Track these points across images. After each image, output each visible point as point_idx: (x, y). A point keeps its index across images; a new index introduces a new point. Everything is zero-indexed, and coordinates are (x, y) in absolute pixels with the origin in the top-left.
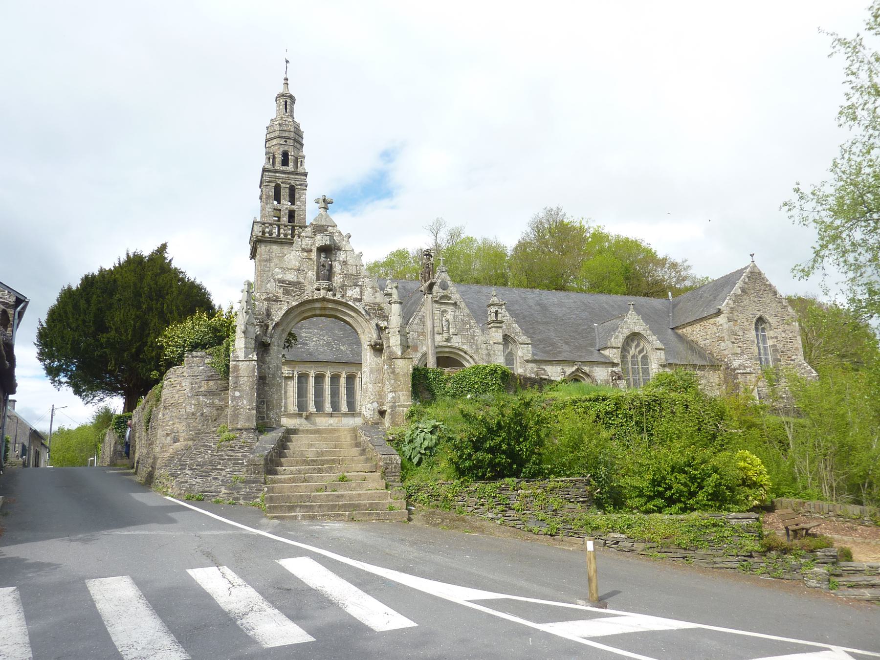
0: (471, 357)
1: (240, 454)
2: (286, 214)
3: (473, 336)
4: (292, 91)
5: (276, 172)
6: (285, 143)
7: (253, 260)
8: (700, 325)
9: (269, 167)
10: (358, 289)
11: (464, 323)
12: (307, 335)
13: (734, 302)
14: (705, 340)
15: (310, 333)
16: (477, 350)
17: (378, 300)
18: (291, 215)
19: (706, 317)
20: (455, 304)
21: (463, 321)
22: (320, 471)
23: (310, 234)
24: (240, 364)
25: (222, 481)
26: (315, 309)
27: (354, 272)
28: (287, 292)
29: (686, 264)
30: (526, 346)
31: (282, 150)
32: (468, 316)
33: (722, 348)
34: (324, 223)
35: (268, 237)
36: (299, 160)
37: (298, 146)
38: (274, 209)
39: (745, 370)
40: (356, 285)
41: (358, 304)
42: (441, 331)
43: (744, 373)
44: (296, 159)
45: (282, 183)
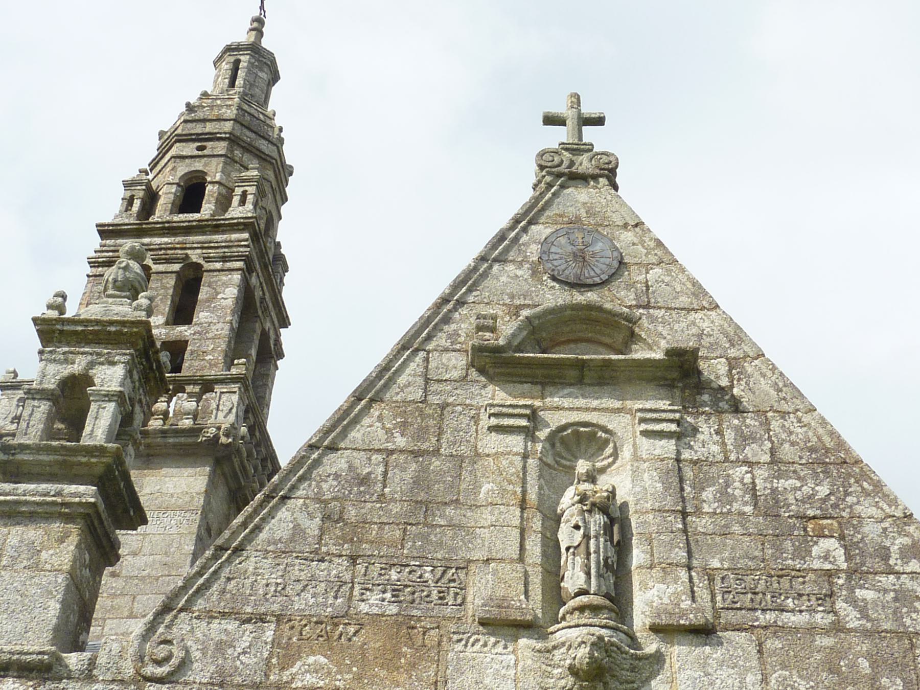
45: (156, 261)
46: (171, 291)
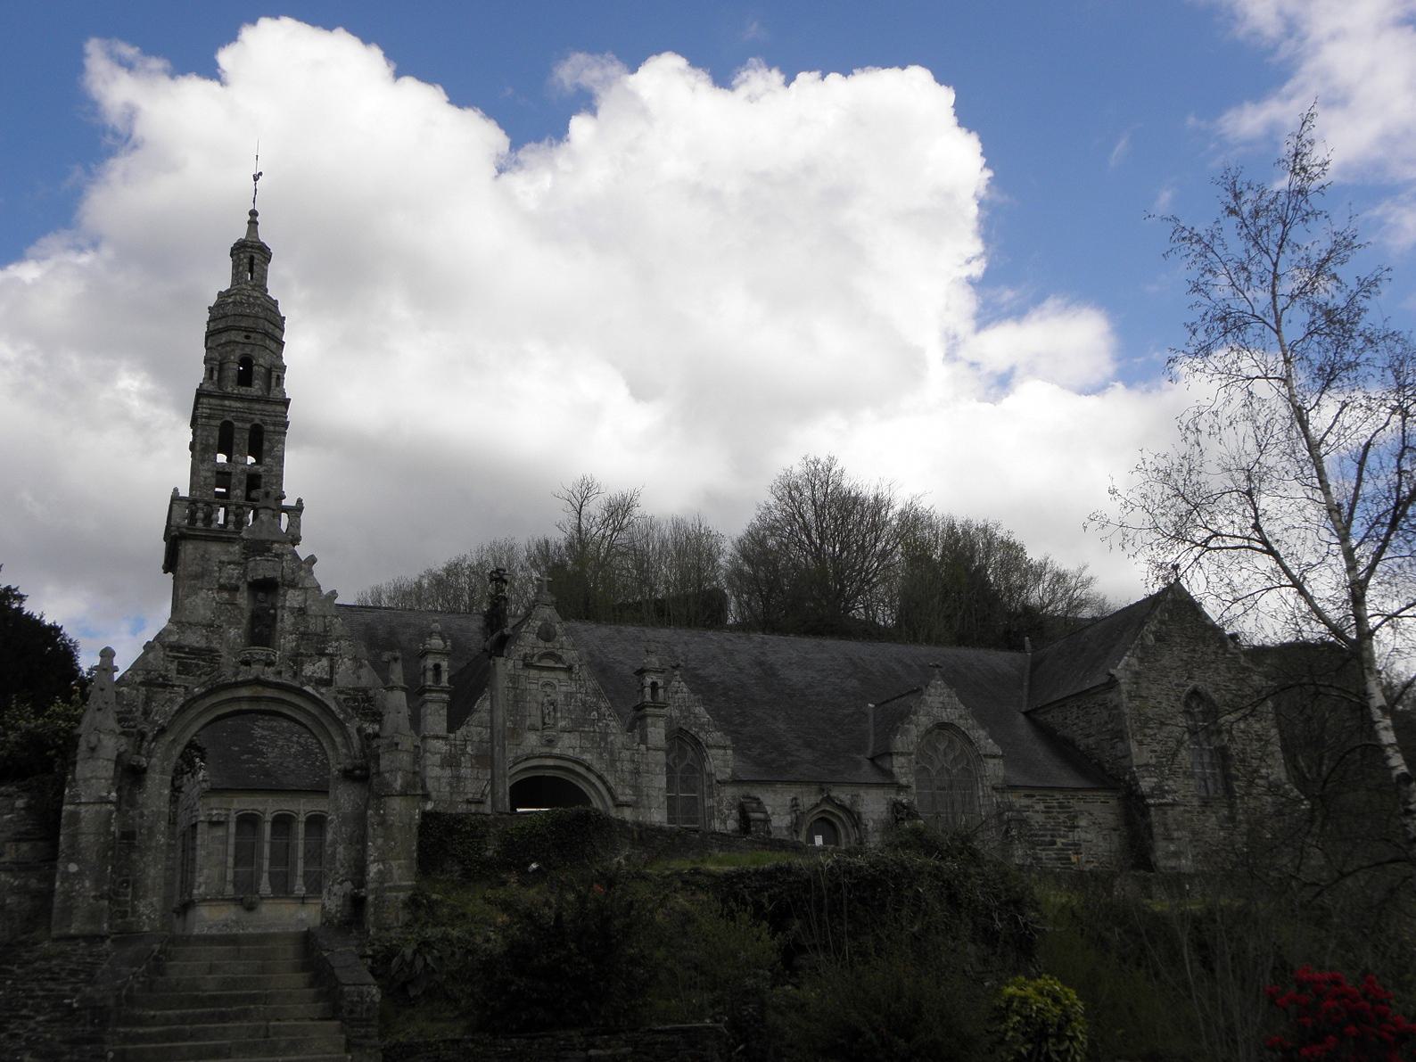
0: (600, 777)
1: (68, 987)
2: (240, 483)
3: (604, 736)
4: (264, 236)
5: (225, 397)
6: (246, 341)
7: (170, 575)
8: (1078, 707)
9: (209, 387)
10: (325, 662)
11: (586, 707)
12: (265, 733)
13: (1141, 660)
14: (1088, 736)
15: (272, 729)
16: (613, 762)
17: (364, 683)
18: (253, 481)
19: (1088, 690)
20: (569, 669)
21: (584, 704)
22: (223, 1017)
23: (236, 558)
24: (83, 809)
25: (28, 1039)
26: (239, 699)
27: (320, 629)
28: (184, 669)
29: (1086, 575)
30: (721, 752)
31: (238, 353)
32: (596, 693)
33: (1119, 754)
34: (264, 536)
35: (201, 530)
36: (274, 375)
37: (273, 346)
38: (218, 473)
39: (1164, 797)
40: (322, 654)
41: (323, 690)
42: (539, 725)
43: (1161, 804)
44: (269, 372)
45: (237, 419)
46: (247, 441)
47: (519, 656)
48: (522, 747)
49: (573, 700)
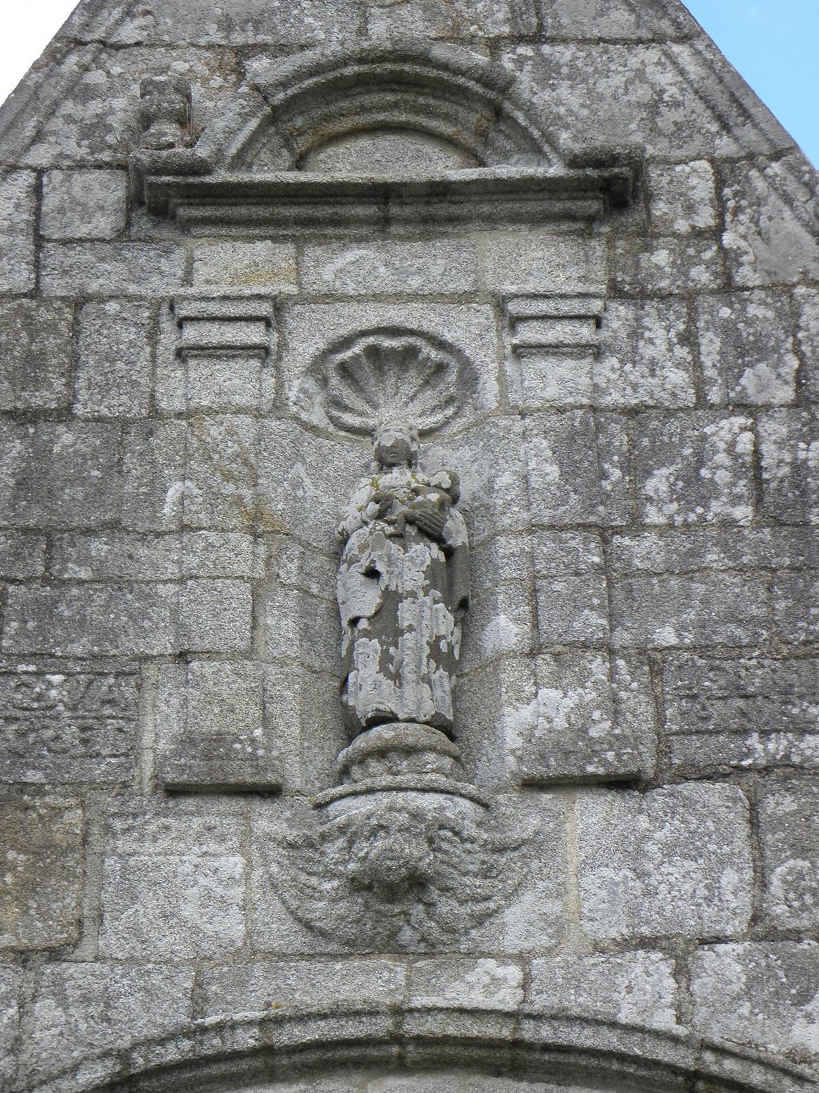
47: (93, 130)
48: (77, 973)
49: (658, 483)
